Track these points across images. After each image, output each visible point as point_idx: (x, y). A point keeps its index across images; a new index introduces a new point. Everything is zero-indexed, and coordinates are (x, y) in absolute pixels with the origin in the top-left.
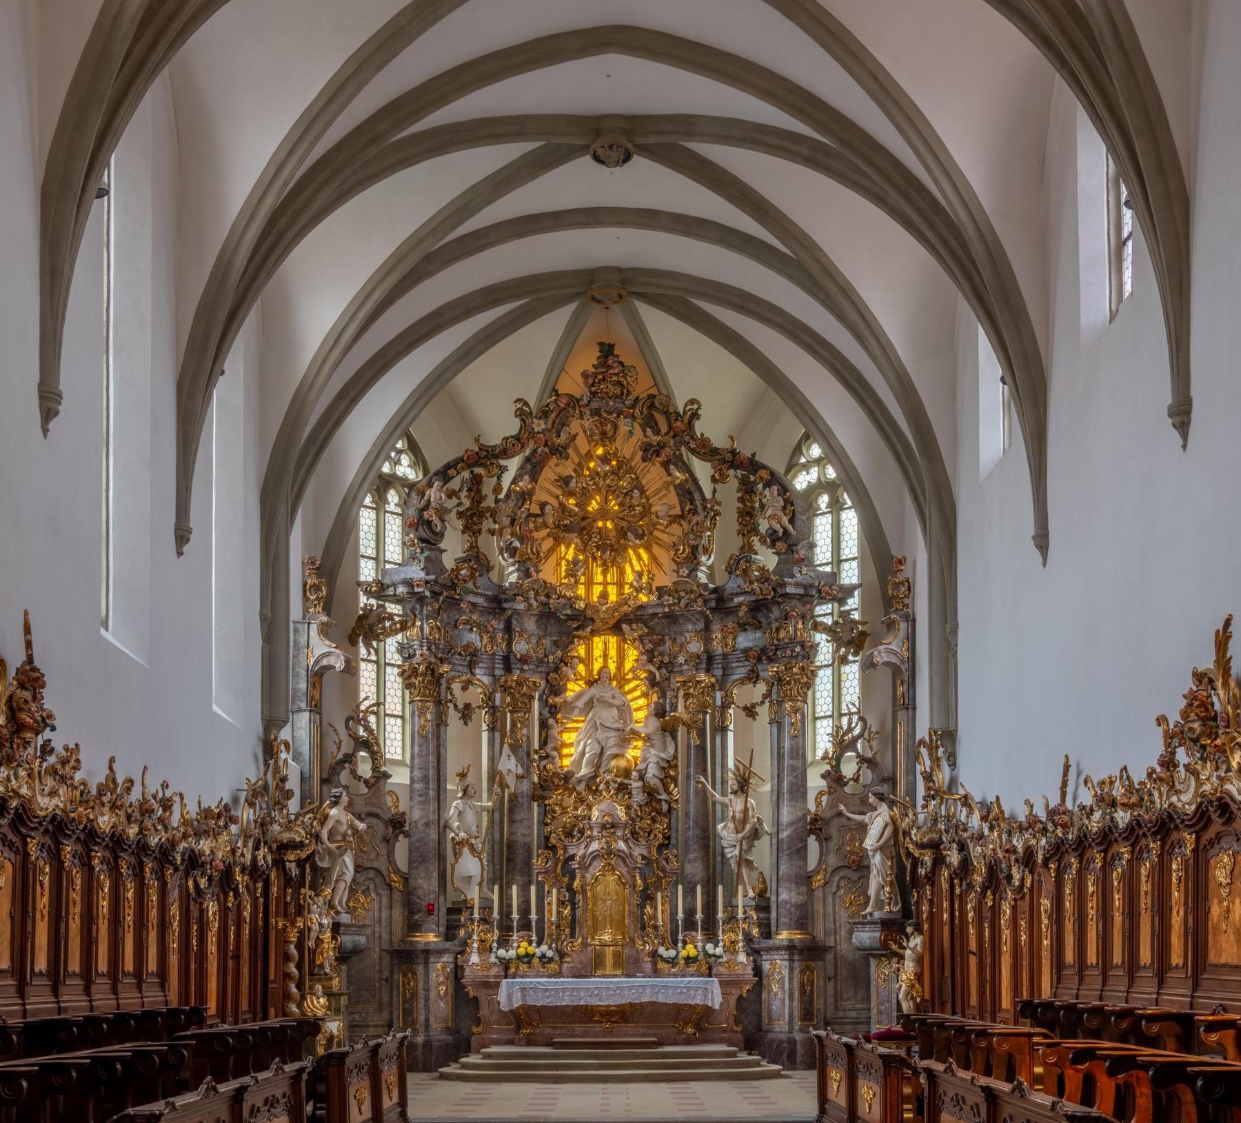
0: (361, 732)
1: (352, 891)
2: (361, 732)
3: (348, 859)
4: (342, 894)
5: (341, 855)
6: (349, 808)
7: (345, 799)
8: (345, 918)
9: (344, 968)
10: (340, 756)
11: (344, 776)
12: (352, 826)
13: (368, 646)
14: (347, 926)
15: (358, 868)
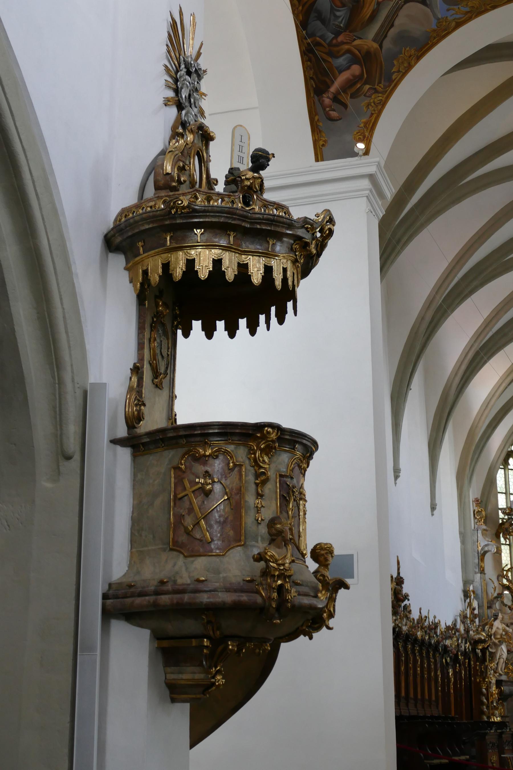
0: (505, 581)
1: (506, 664)
2: (505, 581)
3: (504, 647)
4: (502, 665)
5: (501, 645)
6: (502, 621)
7: (500, 616)
8: (504, 678)
9: (505, 704)
10: (495, 595)
11: (497, 605)
12: (504, 630)
13: (505, 539)
14: (505, 681)
15: (509, 651)
